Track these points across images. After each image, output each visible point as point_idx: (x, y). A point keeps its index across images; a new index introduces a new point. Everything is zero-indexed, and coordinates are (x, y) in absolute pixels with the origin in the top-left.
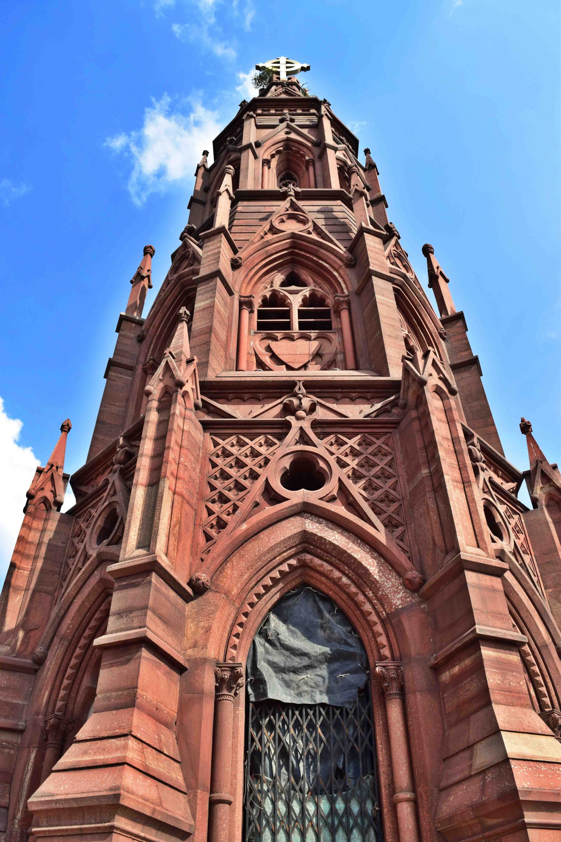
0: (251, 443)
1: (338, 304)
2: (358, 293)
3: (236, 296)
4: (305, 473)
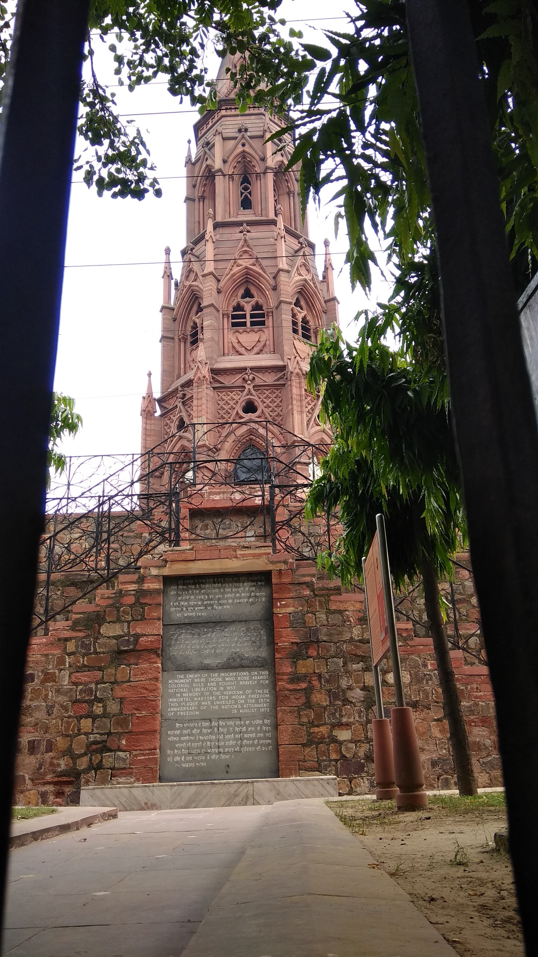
0: (231, 395)
1: (268, 312)
2: (277, 308)
3: (221, 312)
4: (250, 407)
